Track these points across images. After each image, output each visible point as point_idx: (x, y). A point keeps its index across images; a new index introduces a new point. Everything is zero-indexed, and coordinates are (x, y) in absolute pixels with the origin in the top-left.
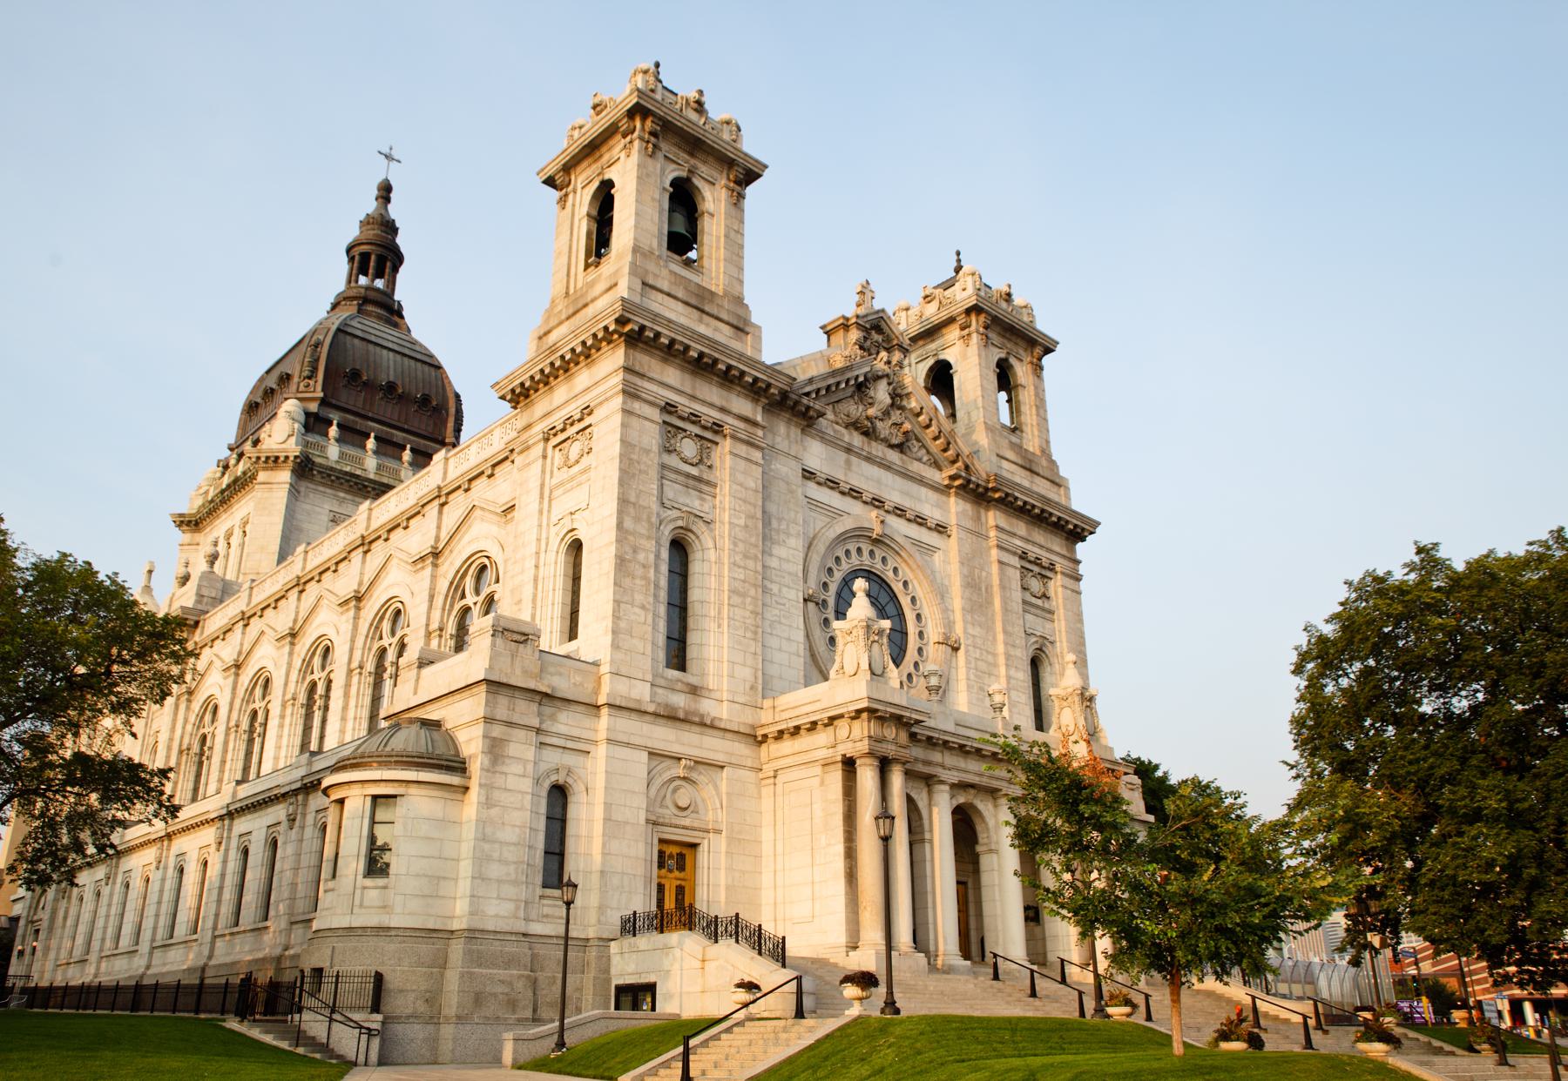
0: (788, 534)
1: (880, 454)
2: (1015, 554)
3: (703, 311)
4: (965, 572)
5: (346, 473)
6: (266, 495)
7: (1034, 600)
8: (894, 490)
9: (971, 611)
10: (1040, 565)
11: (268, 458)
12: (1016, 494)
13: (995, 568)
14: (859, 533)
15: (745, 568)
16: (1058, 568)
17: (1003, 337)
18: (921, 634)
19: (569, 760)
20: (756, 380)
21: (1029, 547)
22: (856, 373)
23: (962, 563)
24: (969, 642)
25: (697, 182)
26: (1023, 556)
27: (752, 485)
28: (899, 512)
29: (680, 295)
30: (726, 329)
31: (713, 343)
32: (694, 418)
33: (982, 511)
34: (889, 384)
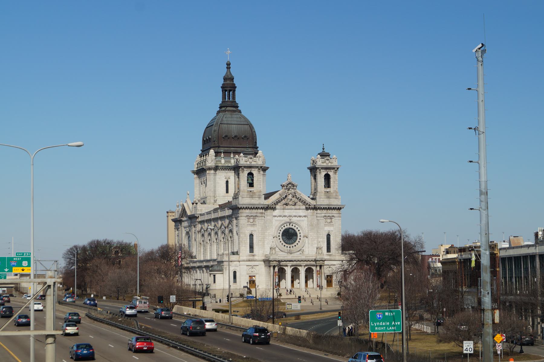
0: (270, 228)
5: (227, 166)
6: (209, 177)
7: (328, 224)
11: (208, 168)
15: (261, 236)
18: (300, 236)
19: (236, 268)
21: (327, 214)
25: (252, 172)
26: (325, 216)
27: (262, 223)
28: (295, 216)
32: (252, 216)
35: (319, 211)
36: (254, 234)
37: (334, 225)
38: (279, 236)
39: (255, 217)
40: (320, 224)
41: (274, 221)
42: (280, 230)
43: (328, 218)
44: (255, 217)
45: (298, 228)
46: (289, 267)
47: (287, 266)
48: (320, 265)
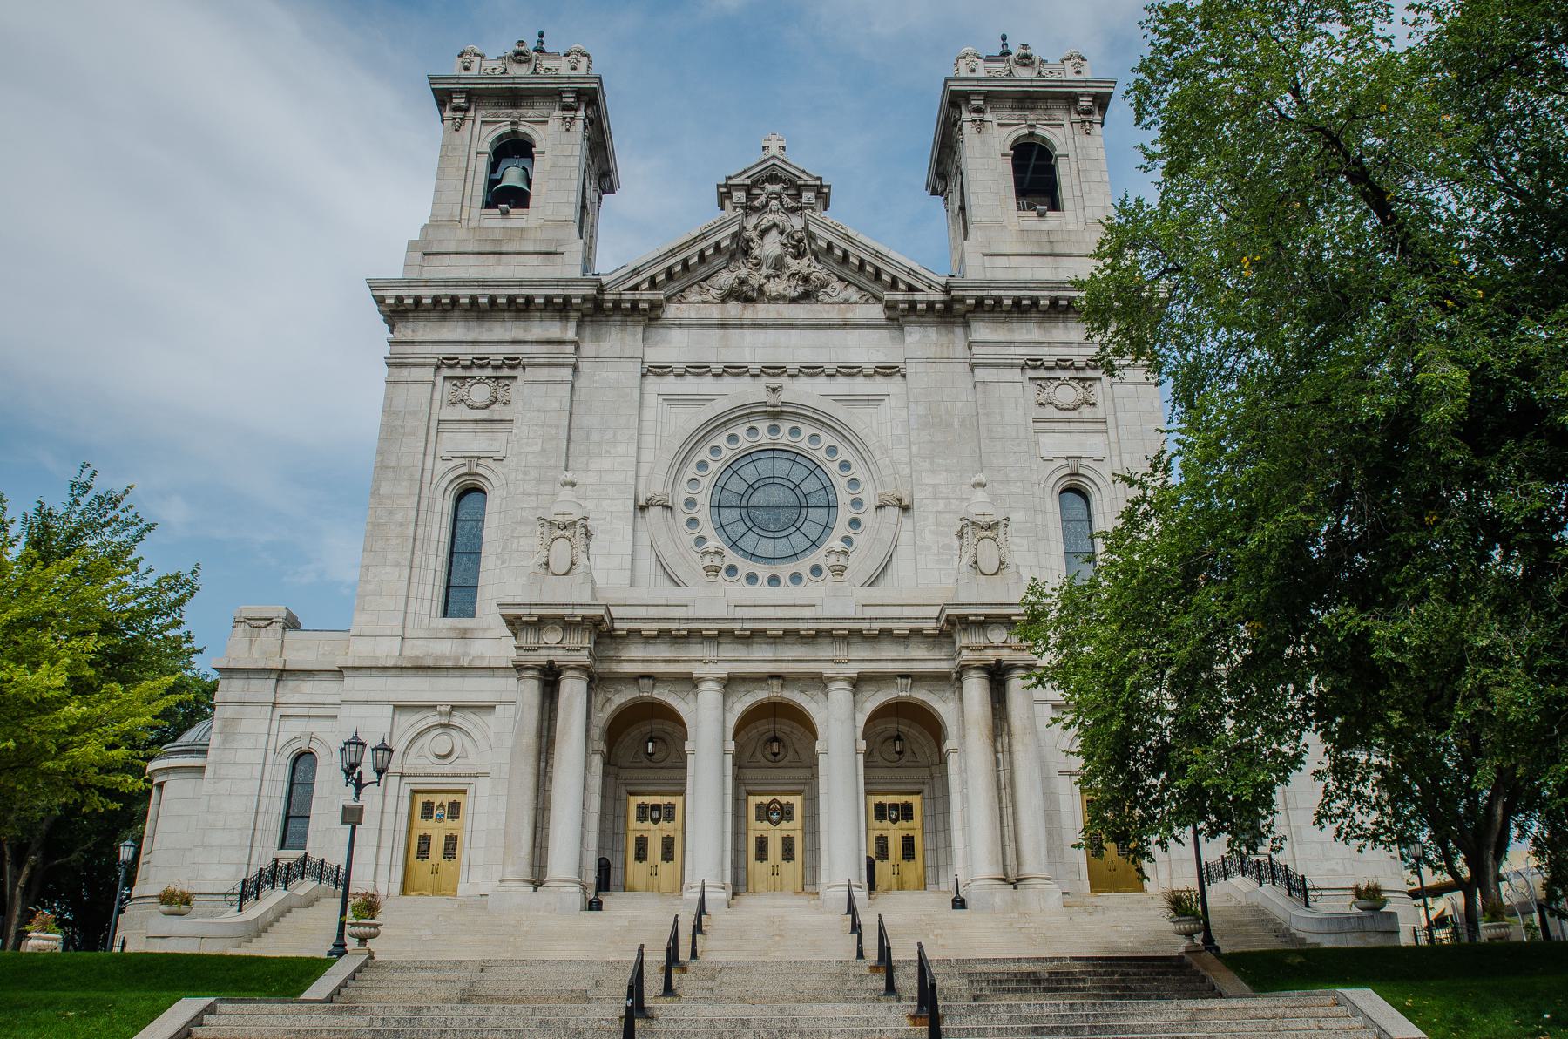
1: (773, 315)
2: (1012, 366)
3: (501, 253)
8: (794, 348)
12: (995, 293)
14: (744, 413)
17: (1022, 109)
18: (857, 503)
20: (549, 300)
22: (713, 240)
25: (522, 129)
26: (1035, 364)
27: (556, 405)
28: (813, 371)
29: (470, 249)
31: (483, 284)
32: (481, 363)
34: (781, 233)
35: (983, 330)
36: (487, 487)
37: (1110, 420)
38: (690, 502)
39: (506, 372)
41: (652, 399)
42: (702, 465)
43: (1059, 373)
44: (506, 372)
45: (840, 449)
46: (709, 695)
47: (690, 682)
48: (986, 668)
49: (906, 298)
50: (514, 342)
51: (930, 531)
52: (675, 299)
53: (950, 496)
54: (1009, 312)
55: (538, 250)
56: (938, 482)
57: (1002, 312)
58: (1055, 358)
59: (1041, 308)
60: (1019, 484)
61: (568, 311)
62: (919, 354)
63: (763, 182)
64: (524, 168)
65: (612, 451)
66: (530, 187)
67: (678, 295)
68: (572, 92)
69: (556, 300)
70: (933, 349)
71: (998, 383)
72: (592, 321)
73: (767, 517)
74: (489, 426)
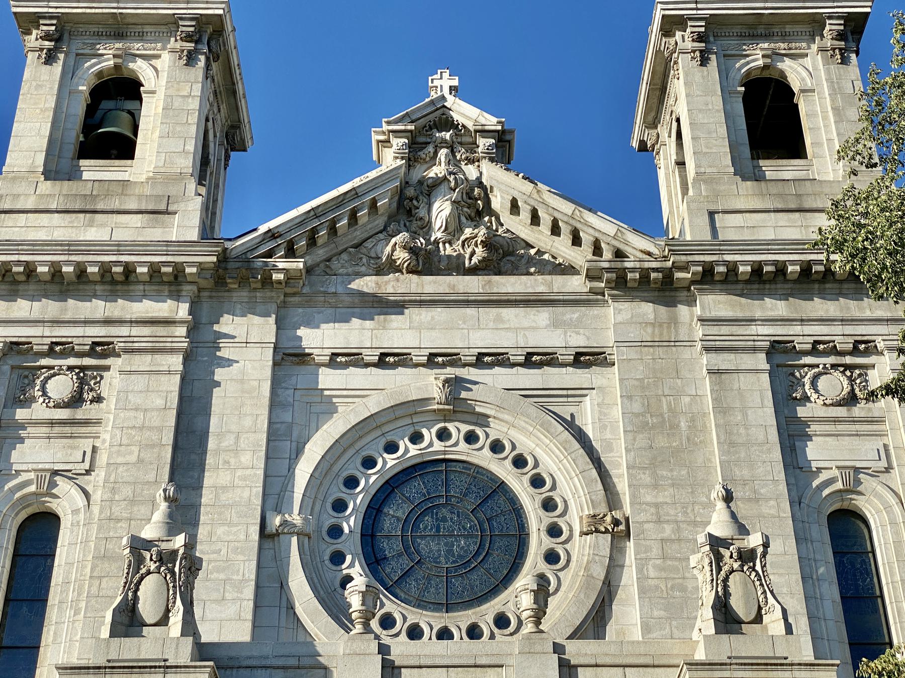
2: (754, 350)
4: (637, 407)
9: (653, 466)
10: (834, 351)
13: (707, 385)
16: (881, 345)
18: (554, 531)
20: (154, 269)
21: (797, 329)
23: (627, 397)
24: (642, 517)
27: (159, 402)
29: (53, 206)
30: (137, 220)
31: (70, 247)
33: (683, 310)
40: (744, 410)
49: (613, 265)
50: (108, 322)
51: (654, 566)
52: (318, 270)
53: (679, 519)
54: (747, 282)
55: (143, 207)
56: (660, 500)
57: (737, 282)
58: (811, 340)
59: (789, 277)
60: (772, 503)
61: (180, 284)
62: (631, 336)
63: (431, 128)
64: (130, 113)
65: (232, 461)
66: (136, 135)
67: (322, 265)
68: (191, 19)
69: (164, 269)
70: (649, 330)
71: (738, 371)
72: (210, 297)
73: (435, 548)
74: (67, 430)
